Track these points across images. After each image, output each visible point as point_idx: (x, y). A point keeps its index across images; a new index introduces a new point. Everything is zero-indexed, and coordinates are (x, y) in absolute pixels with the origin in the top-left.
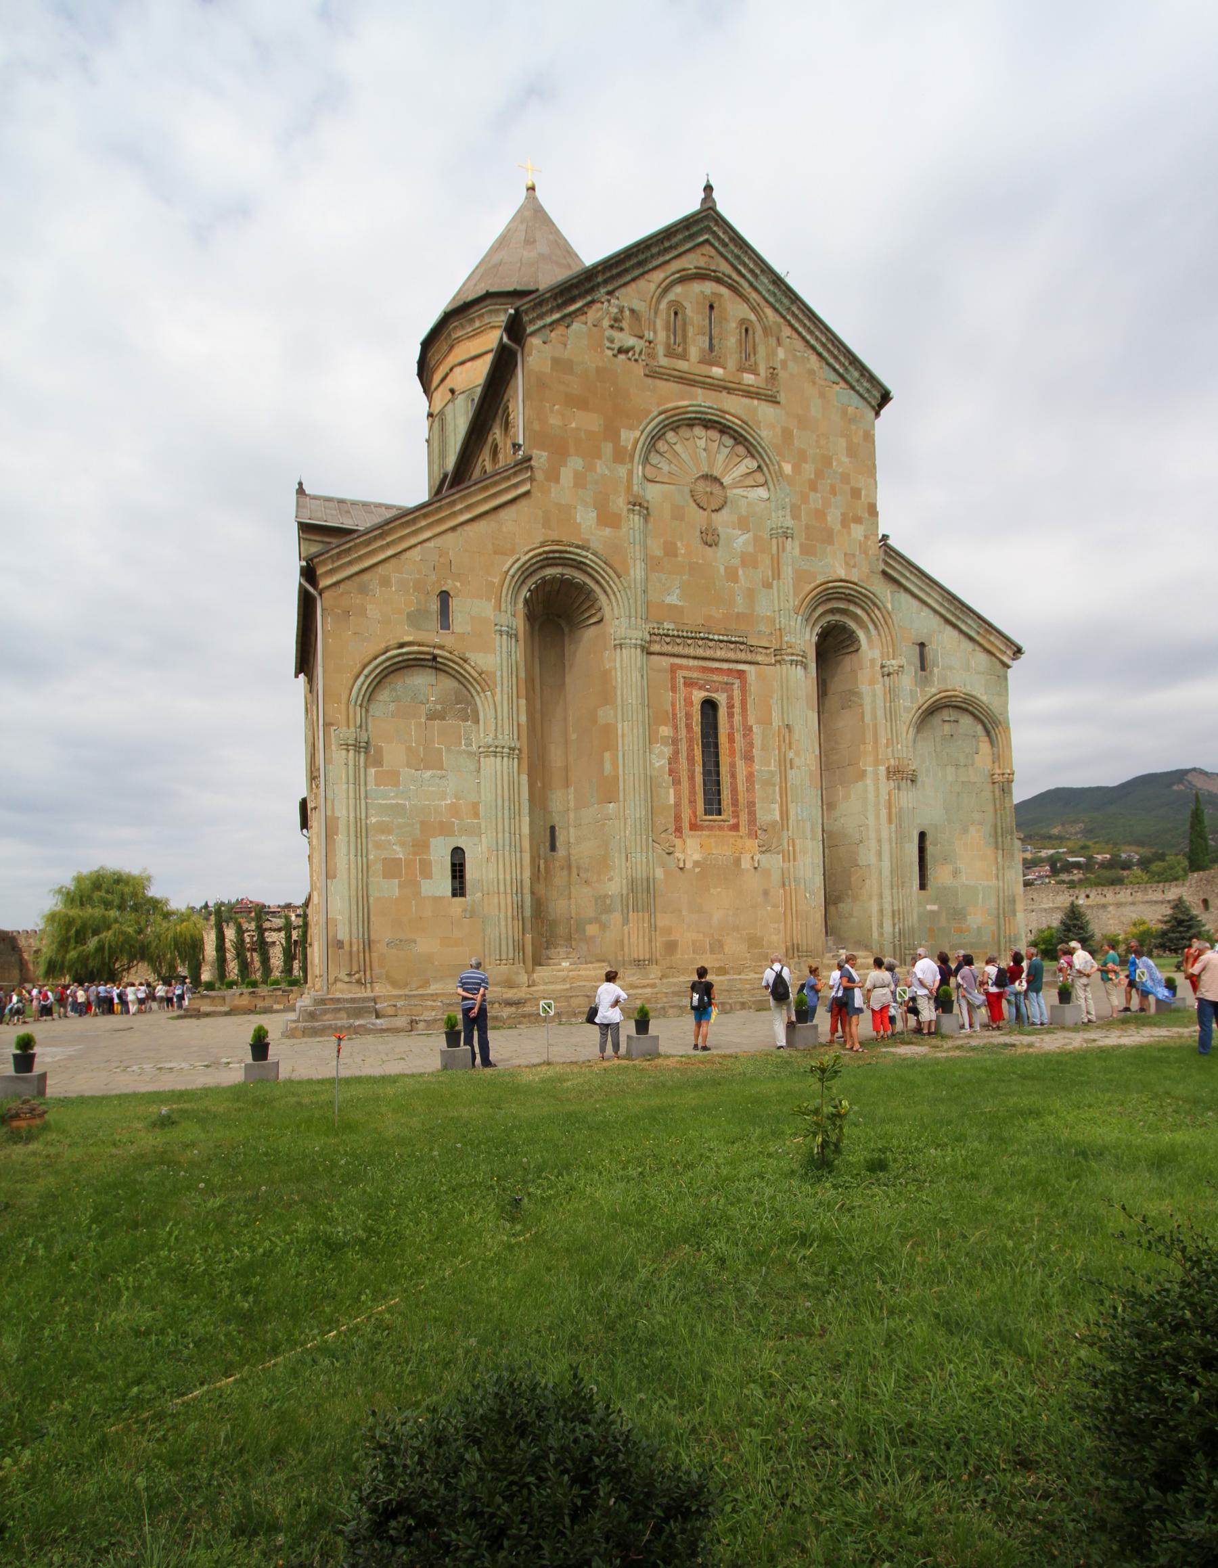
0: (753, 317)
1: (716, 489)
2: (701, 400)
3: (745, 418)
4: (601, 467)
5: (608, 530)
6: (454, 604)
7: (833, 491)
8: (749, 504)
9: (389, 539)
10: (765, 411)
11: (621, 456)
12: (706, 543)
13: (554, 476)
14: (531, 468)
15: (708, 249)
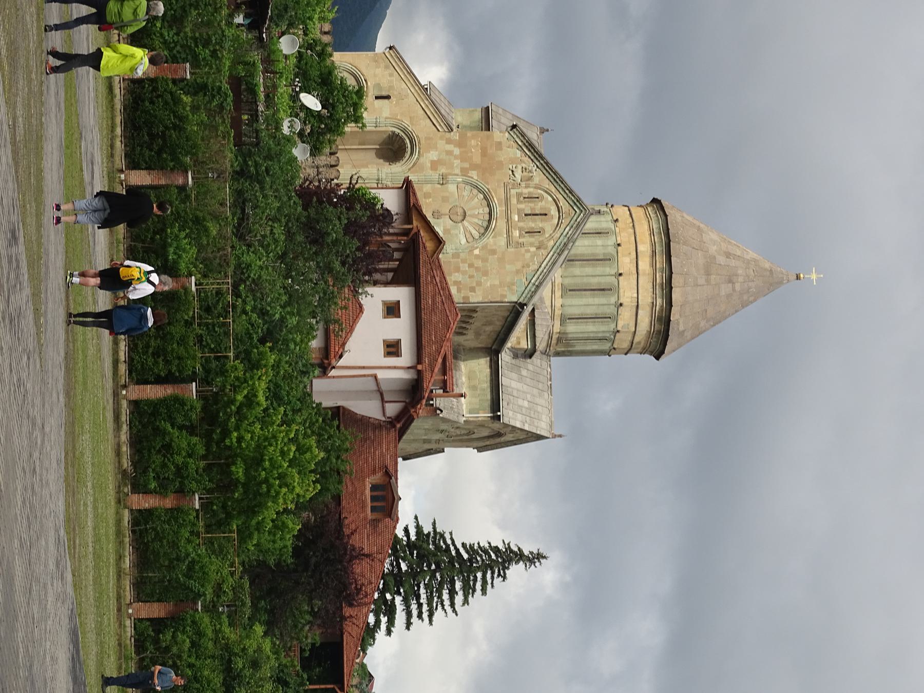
0: (547, 236)
1: (460, 218)
2: (499, 209)
3: (496, 230)
4: (457, 162)
5: (430, 165)
6: (386, 101)
7: (471, 277)
8: (457, 235)
9: (408, 76)
10: (502, 241)
11: (464, 172)
12: (433, 212)
13: (449, 141)
14: (450, 132)
15: (574, 212)
